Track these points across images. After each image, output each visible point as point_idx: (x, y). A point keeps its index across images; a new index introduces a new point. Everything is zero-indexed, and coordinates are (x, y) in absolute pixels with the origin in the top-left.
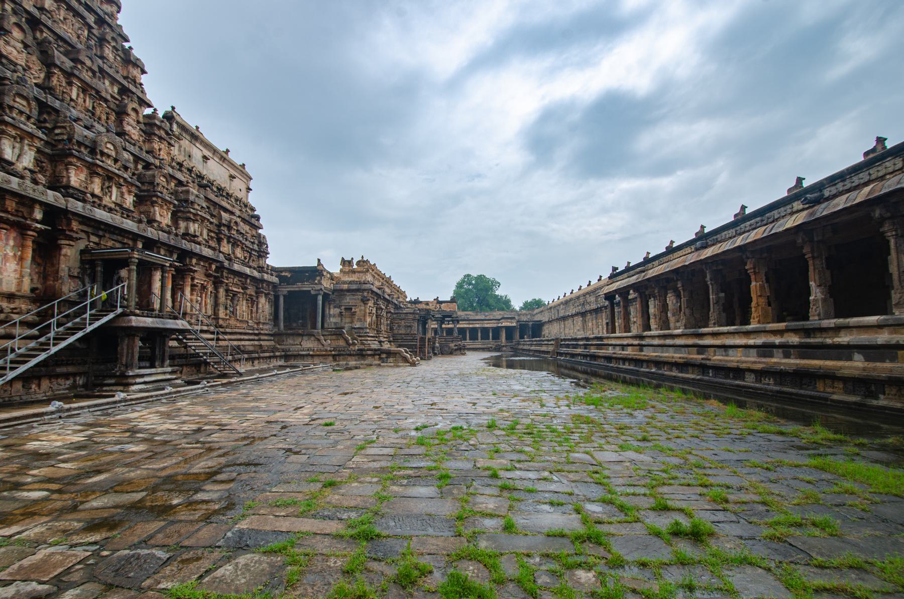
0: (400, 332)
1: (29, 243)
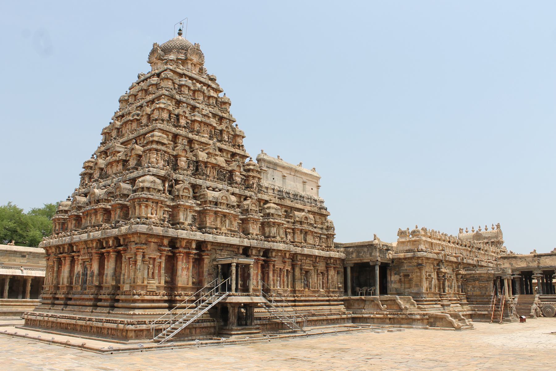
0: (475, 293)
1: (191, 260)
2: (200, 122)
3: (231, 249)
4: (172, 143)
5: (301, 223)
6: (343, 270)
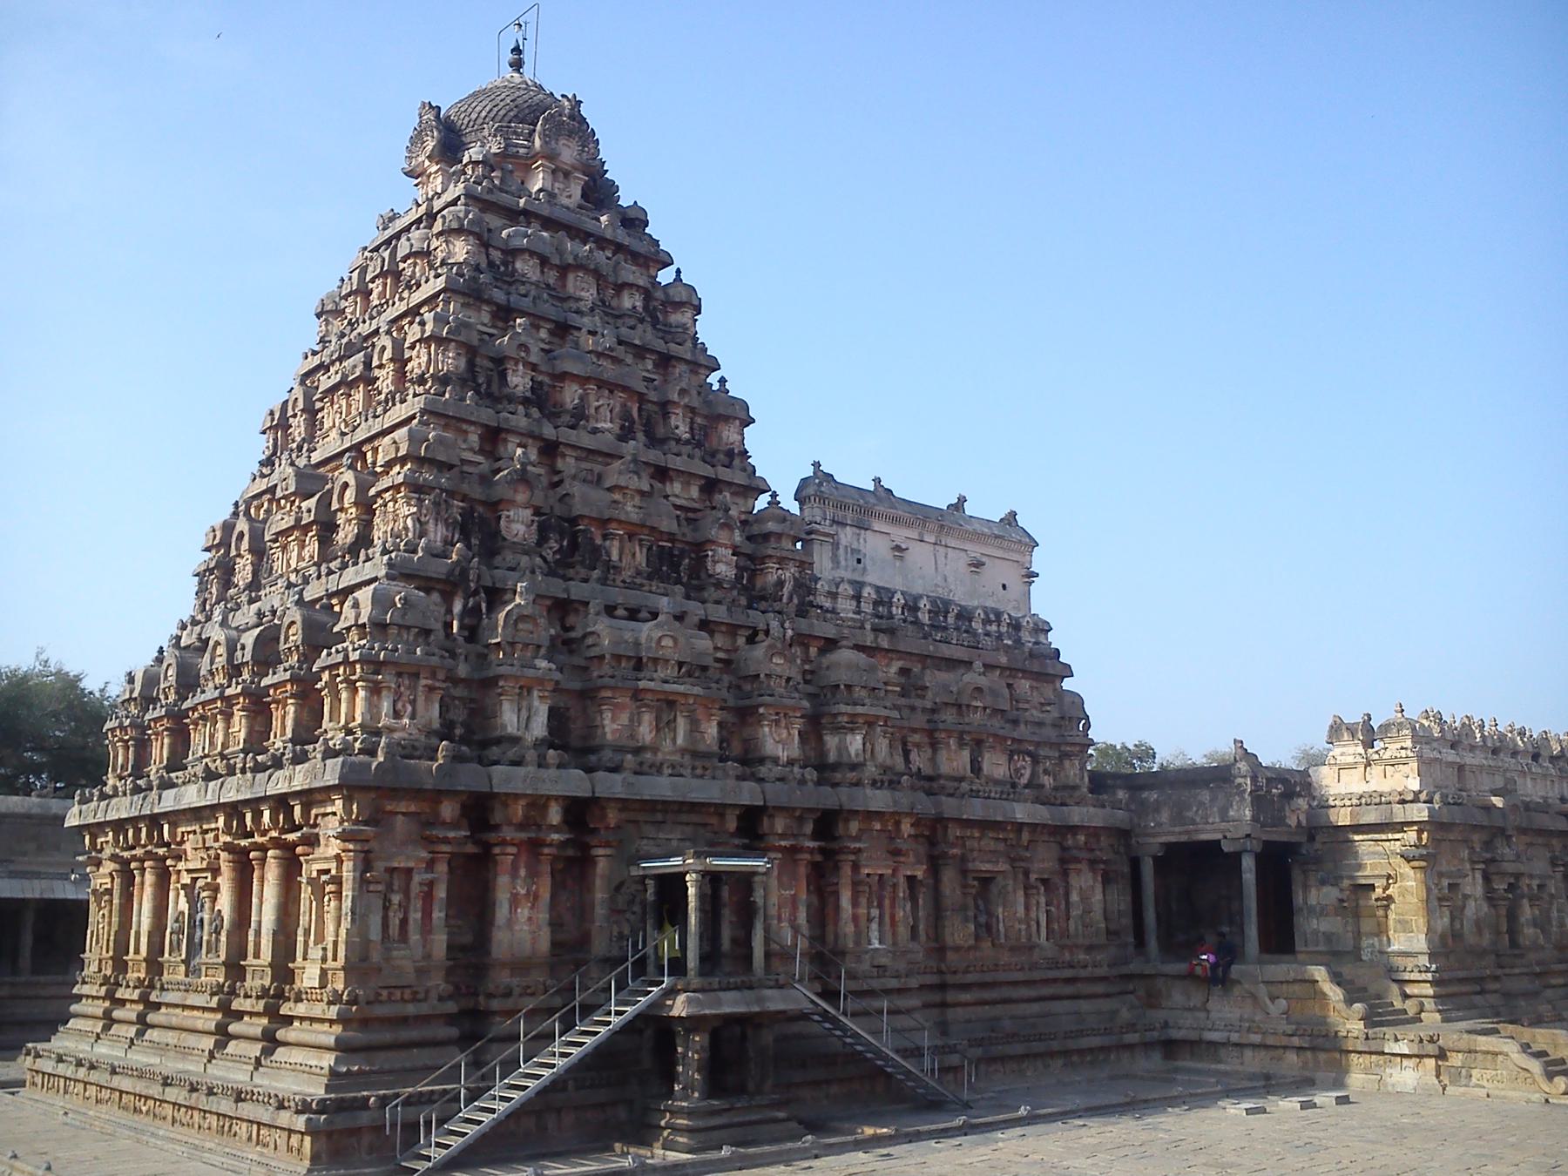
1: (546, 868)
3: (695, 818)
4: (480, 458)
6: (1126, 869)
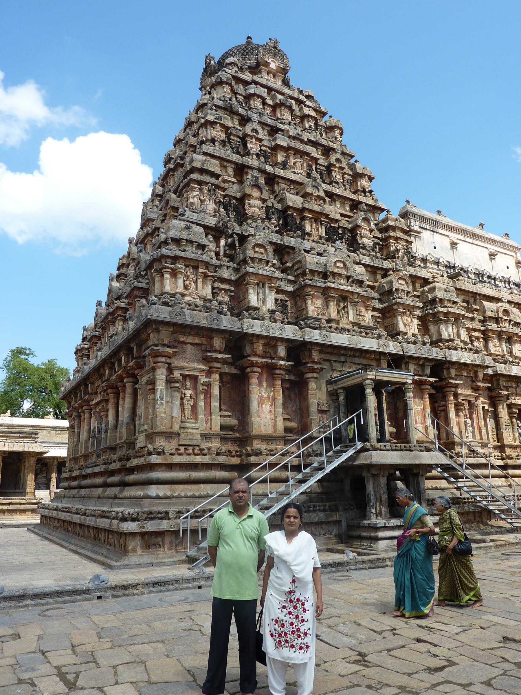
2: (286, 149)
5: (497, 320)
